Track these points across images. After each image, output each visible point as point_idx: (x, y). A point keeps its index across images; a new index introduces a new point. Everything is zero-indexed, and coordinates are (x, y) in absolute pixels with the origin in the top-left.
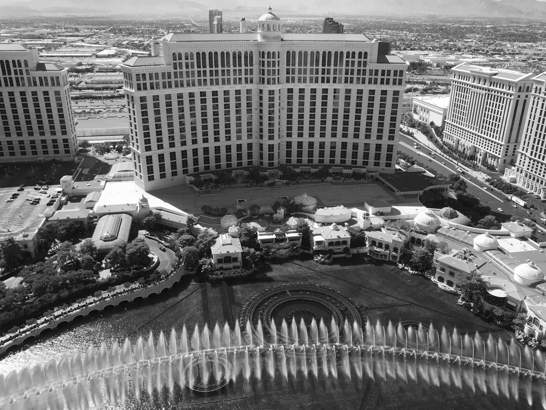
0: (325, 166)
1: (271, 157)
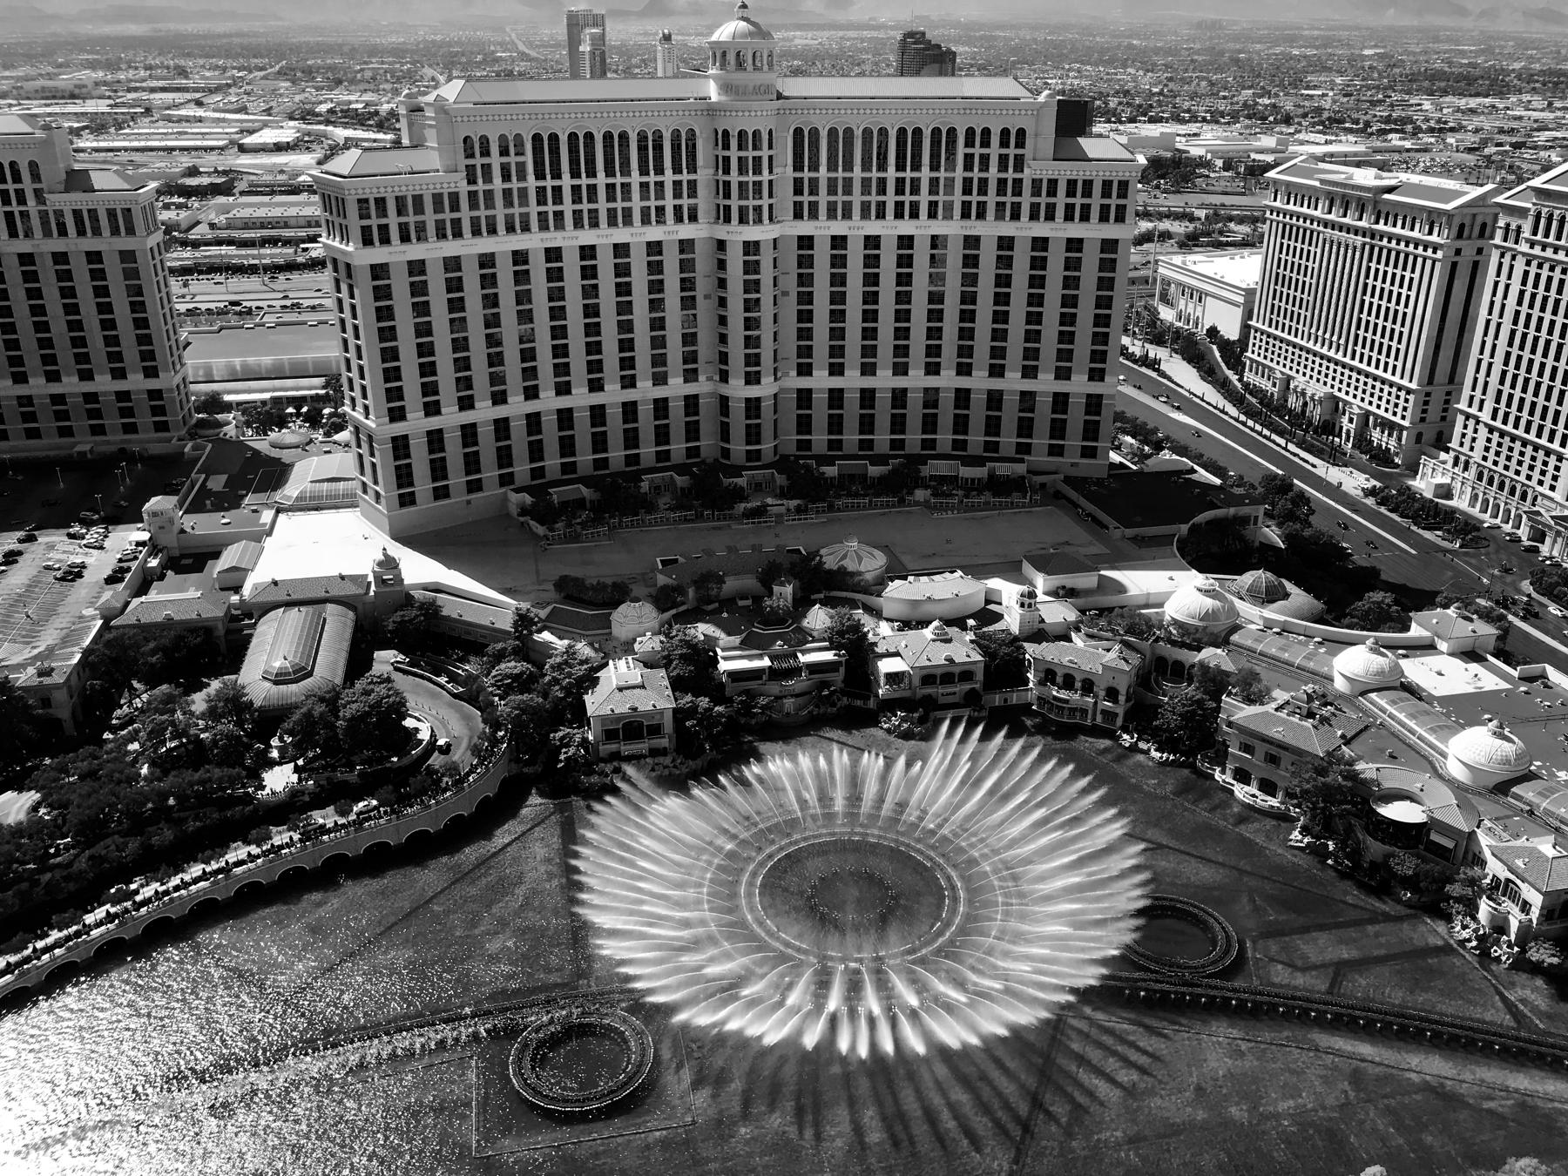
1: (753, 435)
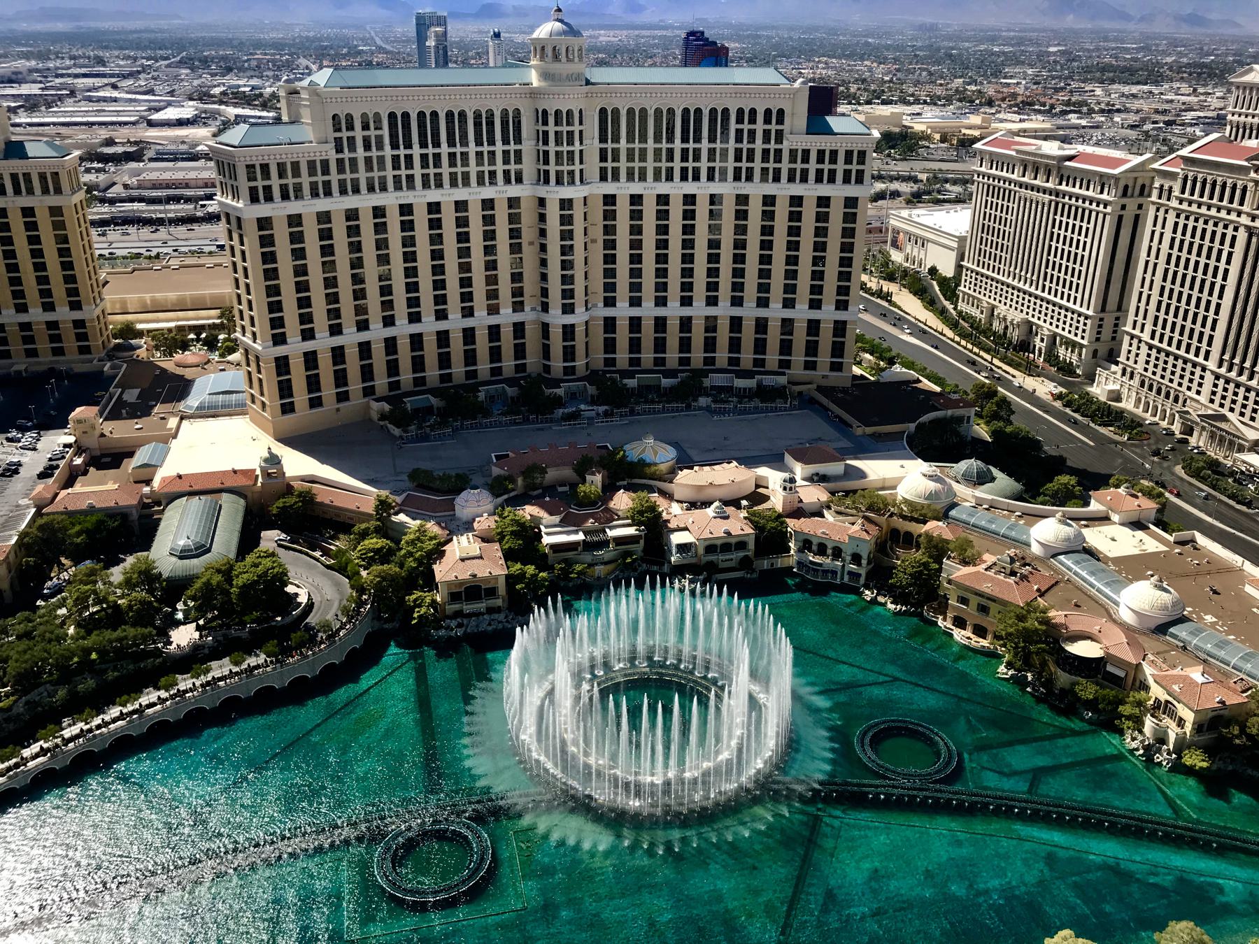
0: (691, 371)
1: (569, 354)
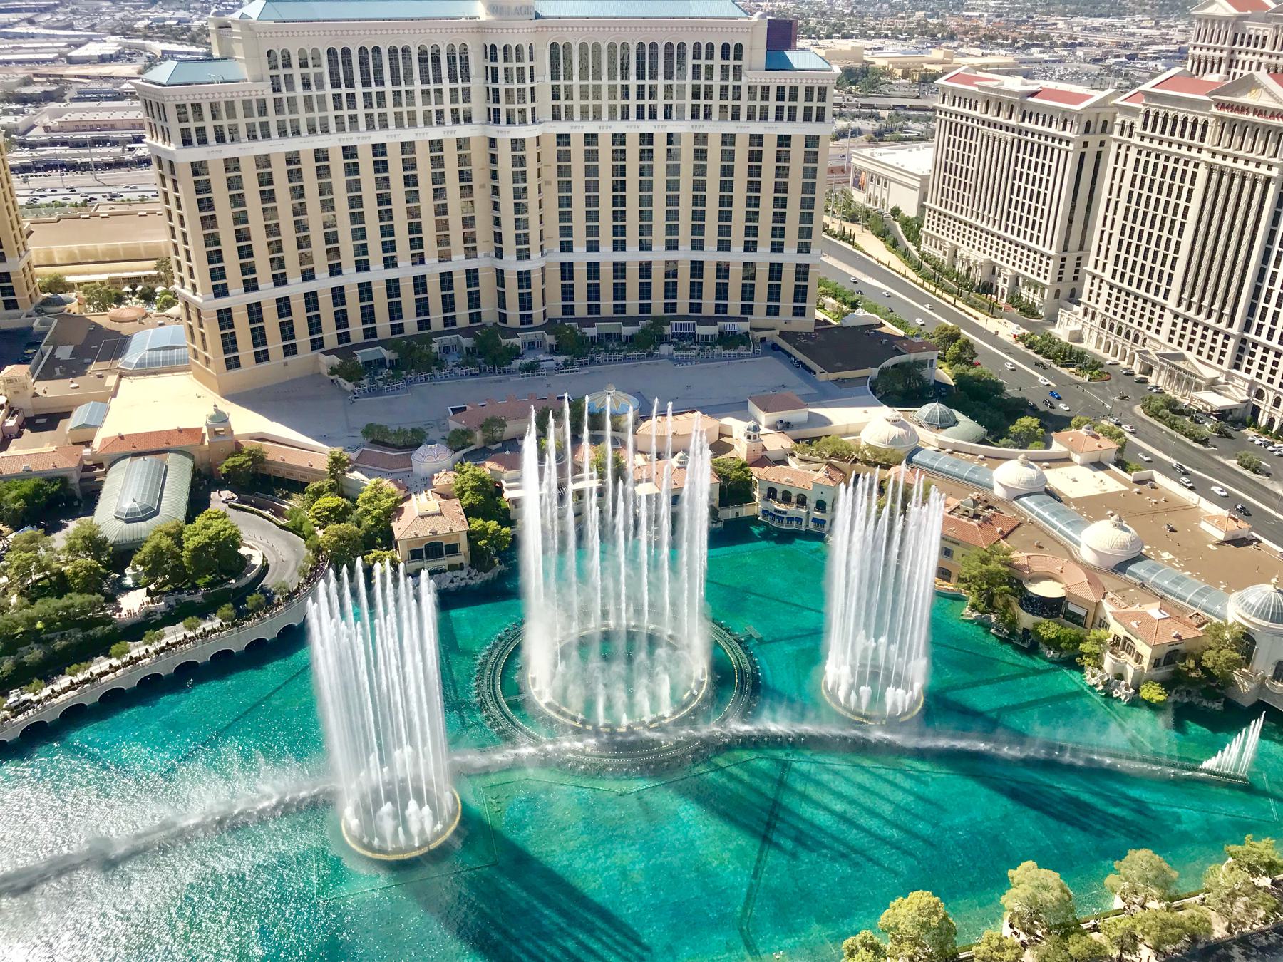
0: (654, 318)
1: (525, 302)
